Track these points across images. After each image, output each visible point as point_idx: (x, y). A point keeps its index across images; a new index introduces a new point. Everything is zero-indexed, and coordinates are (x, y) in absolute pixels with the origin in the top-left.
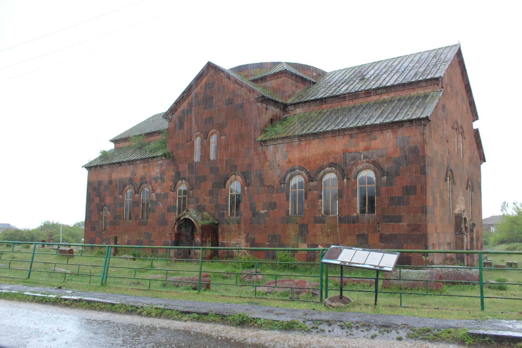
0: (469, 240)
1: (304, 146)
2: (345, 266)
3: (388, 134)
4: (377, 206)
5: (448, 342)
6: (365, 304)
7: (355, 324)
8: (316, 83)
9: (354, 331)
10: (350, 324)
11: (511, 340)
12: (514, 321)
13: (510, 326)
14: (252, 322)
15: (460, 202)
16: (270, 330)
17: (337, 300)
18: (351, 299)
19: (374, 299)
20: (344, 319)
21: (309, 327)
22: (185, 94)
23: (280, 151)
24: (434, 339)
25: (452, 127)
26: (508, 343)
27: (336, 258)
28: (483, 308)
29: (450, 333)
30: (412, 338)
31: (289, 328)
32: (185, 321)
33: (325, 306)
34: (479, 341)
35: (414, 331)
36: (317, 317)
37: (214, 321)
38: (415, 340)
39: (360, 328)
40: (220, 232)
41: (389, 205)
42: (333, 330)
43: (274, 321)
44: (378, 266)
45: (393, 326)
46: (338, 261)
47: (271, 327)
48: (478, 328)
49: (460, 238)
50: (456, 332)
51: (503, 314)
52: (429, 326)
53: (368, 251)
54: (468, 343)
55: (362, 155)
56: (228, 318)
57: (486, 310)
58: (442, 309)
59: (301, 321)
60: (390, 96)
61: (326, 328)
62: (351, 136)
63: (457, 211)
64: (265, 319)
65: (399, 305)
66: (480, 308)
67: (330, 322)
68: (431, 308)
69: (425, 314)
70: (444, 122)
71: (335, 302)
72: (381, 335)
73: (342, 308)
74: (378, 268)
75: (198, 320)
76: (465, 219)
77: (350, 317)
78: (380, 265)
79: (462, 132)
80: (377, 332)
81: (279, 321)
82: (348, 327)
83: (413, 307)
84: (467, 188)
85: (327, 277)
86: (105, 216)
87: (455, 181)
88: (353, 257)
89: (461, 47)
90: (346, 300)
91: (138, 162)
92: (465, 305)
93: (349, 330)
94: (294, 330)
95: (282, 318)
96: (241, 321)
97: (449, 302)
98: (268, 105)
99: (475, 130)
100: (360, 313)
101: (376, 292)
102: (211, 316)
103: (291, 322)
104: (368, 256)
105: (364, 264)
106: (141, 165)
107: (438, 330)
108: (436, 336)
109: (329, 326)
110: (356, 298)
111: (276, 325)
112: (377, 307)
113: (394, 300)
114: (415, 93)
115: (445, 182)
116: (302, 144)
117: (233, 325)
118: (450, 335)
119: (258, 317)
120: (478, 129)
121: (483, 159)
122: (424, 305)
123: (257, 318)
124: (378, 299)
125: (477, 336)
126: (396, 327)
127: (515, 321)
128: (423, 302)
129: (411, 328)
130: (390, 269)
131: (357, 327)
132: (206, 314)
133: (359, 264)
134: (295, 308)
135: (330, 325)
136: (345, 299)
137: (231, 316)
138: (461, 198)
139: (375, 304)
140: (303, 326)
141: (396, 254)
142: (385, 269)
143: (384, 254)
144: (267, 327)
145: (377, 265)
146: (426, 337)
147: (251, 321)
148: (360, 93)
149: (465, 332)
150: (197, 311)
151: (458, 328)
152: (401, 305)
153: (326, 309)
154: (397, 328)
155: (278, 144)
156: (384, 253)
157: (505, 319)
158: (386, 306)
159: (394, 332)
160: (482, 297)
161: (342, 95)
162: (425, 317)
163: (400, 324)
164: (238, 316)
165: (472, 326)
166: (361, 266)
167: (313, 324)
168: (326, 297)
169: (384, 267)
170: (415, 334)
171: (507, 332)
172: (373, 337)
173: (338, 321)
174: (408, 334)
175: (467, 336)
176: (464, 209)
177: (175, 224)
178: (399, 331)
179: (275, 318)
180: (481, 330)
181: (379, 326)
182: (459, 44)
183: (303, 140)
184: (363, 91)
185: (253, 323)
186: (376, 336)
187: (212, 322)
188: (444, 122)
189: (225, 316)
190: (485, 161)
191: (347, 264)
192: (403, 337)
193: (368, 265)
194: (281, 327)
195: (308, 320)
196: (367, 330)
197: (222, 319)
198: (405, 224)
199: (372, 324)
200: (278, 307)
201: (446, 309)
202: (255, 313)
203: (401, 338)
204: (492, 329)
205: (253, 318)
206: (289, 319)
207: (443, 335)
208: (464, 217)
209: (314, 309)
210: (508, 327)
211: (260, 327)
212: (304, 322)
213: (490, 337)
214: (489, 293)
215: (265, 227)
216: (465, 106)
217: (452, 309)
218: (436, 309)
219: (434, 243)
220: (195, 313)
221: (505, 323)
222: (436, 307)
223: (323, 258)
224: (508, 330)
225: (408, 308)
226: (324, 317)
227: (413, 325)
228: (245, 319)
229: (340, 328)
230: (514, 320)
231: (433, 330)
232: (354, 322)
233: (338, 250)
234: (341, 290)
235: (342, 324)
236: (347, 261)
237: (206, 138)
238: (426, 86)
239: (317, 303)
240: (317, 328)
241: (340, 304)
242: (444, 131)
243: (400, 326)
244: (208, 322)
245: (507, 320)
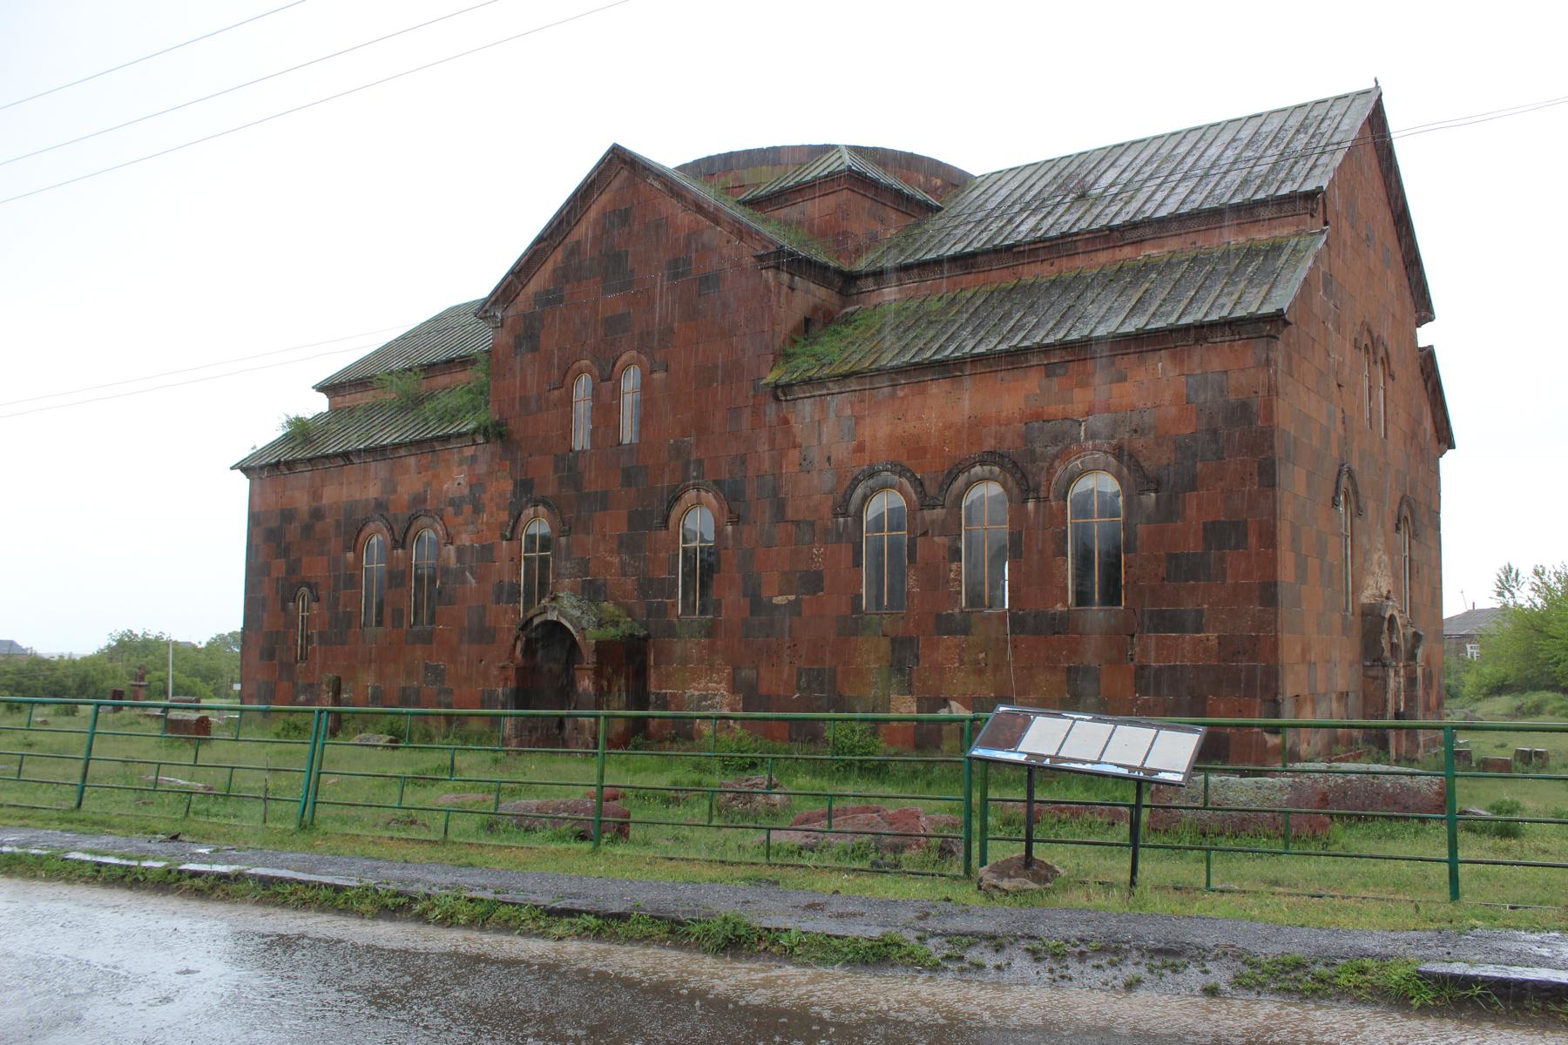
0: (1402, 685)
2: (1040, 767)
3: (1160, 364)
4: (1127, 583)
5: (1357, 1001)
6: (1100, 883)
7: (1075, 946)
8: (941, 209)
9: (1074, 968)
10: (1061, 945)
11: (1548, 994)
12: (1552, 934)
13: (1545, 952)
14: (764, 941)
15: (1377, 570)
16: (819, 964)
17: (1016, 871)
18: (1057, 867)
19: (1128, 866)
20: (1041, 930)
21: (937, 957)
22: (545, 244)
23: (832, 415)
24: (1314, 991)
26: (1539, 1005)
27: (1012, 744)
28: (1455, 894)
29: (1362, 971)
30: (1250, 988)
31: (874, 959)
32: (560, 939)
33: (980, 888)
34: (1450, 998)
35: (1253, 965)
36: (960, 924)
37: (646, 940)
38: (1259, 993)
39: (1092, 957)
40: (652, 663)
41: (1163, 579)
42: (1009, 964)
43: (828, 936)
44: (1141, 769)
45: (1189, 953)
46: (1021, 752)
47: (819, 955)
48: (1447, 958)
49: (1375, 678)
50: (1381, 969)
51: (1517, 912)
52: (1298, 952)
53: (1111, 722)
54: (1418, 1004)
55: (1083, 428)
56: (691, 929)
57: (1466, 898)
58: (1333, 897)
59: (910, 936)
60: (1166, 249)
61: (990, 959)
63: (1366, 597)
64: (804, 933)
65: (1203, 885)
66: (1448, 897)
67: (999, 940)
68: (1298, 895)
69: (1282, 911)
70: (1330, 326)
71: (1010, 877)
72: (1155, 977)
73: (1032, 895)
74: (1142, 774)
75: (598, 935)
76: (1392, 616)
77: (1058, 923)
78: (1148, 765)
79: (1384, 356)
80: (1142, 971)
81: (844, 937)
82: (1055, 955)
83: (1244, 892)
84: (1398, 528)
85: (985, 801)
86: (303, 617)
87: (1361, 504)
88: (1065, 739)
89: (1384, 98)
90: (1043, 872)
91: (403, 452)
92: (1400, 885)
93: (1059, 963)
94: (892, 965)
95: (855, 930)
96: (730, 936)
97: (1352, 875)
98: (797, 278)
99: (1422, 350)
100: (1089, 911)
101: (1135, 843)
102: (639, 923)
103: (883, 940)
104: (1110, 738)
105: (1098, 762)
106: (412, 461)
107: (1326, 965)
108: (1323, 981)
109: (997, 951)
110: (1071, 864)
111: (836, 951)
112: (1137, 891)
113: (1186, 869)
114: (1242, 239)
115: (1333, 510)
116: (900, 394)
117: (705, 951)
118: (1363, 977)
119: (782, 926)
120: (1431, 347)
121: (1445, 439)
122: (1276, 883)
123: (777, 929)
124: (1140, 866)
125: (1445, 983)
126: (1201, 955)
127: (1557, 934)
128: (1271, 875)
129: (1245, 957)
130: (1179, 778)
131: (1082, 953)
132: (622, 917)
133: (1084, 762)
134: (890, 895)
135: (999, 948)
136: (1041, 867)
137: (700, 921)
138: (1380, 557)
139: (1133, 883)
140: (919, 952)
141: (1196, 732)
142: (1162, 776)
143: (1158, 732)
144: (810, 955)
145: (1138, 765)
146: (1291, 985)
147: (760, 939)
148: (1074, 239)
149: (1409, 970)
150: (596, 908)
151: (1387, 957)
152: (1208, 884)
153: (984, 899)
154: (1204, 957)
155: (828, 394)
156: (1160, 727)
157: (1526, 930)
158: (1165, 888)
159: (1193, 970)
160: (1453, 862)
162: (1286, 923)
163: (1211, 945)
164: (719, 922)
165: (1428, 952)
166: (1088, 767)
167: (947, 945)
168: (983, 862)
169: (1161, 771)
170: (1257, 976)
171: (1537, 969)
172: (1130, 986)
173: (1022, 937)
174: (1235, 977)
175: (1415, 984)
176: (1389, 592)
177: (517, 638)
178: (1208, 966)
179: (834, 927)
180: (1460, 964)
181: (1150, 951)
182: (1377, 86)
183: (903, 382)
184: (1083, 234)
185: (767, 944)
186: (1139, 981)
187: (640, 940)
188: (1330, 326)
189: (680, 923)
191: (1047, 761)
192: (1223, 986)
193: (1111, 764)
194: (851, 956)
195: (934, 935)
196: (1113, 964)
197: (672, 932)
198: (1213, 636)
199: (1127, 946)
200: (836, 892)
201: (1343, 898)
202: (772, 913)
203: (1216, 989)
204: (1490, 960)
205: (766, 929)
206: (876, 932)
207: (1342, 980)
208: (1387, 616)
209: (948, 900)
210: (1538, 953)
211: (788, 955)
212: (919, 938)
213: (1485, 985)
214: (1470, 848)
216: (1393, 279)
217: (1363, 898)
218: (1313, 897)
219: (1299, 692)
220: (588, 913)
221: (1528, 941)
222: (1312, 891)
223: (974, 745)
224: (1539, 964)
225: (1229, 896)
226: (979, 925)
227: (1252, 949)
228: (742, 931)
229: (1029, 957)
230: (1553, 931)
231: (1313, 963)
232: (1073, 940)
233: (1020, 721)
234: (1029, 841)
235: (1036, 944)
236: (1046, 753)
237: (609, 379)
238: (1278, 218)
239: (955, 878)
240: (961, 958)
241: (1026, 883)
242: (1329, 355)
243: (1211, 951)
244: (630, 940)
245: (1533, 932)
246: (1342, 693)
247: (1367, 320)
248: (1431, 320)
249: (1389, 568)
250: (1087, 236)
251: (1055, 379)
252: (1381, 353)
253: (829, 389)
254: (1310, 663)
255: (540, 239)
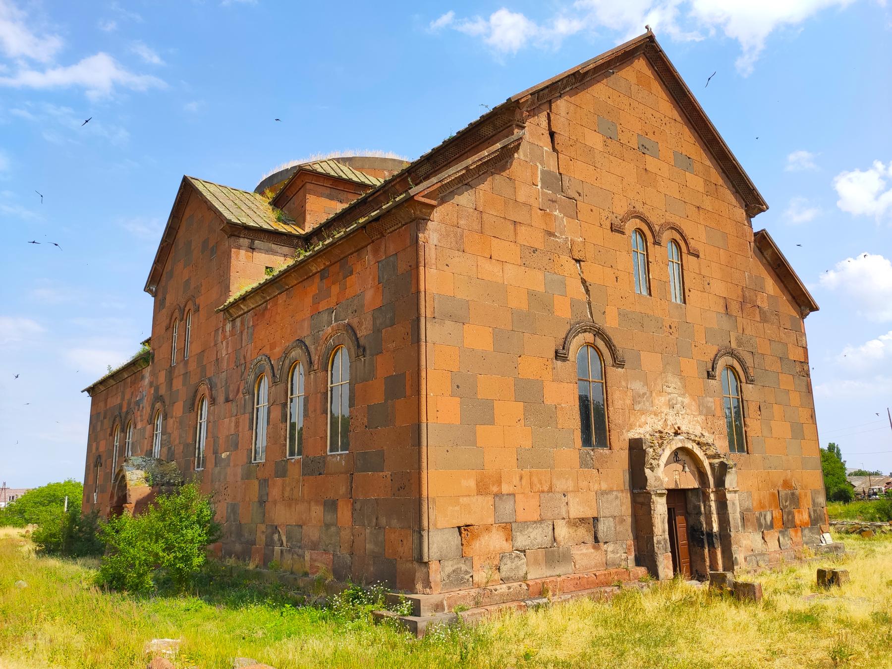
1: (270, 312)
3: (367, 257)
25: (609, 227)
49: (642, 504)
55: (334, 314)
62: (323, 274)
63: (634, 434)
70: (557, 213)
79: (678, 237)
98: (256, 241)
115: (559, 363)
138: (669, 401)
161: (369, 197)
188: (557, 213)
190: (814, 308)
198: (388, 473)
215: (225, 489)
246: (582, 520)
247: (639, 208)
248: (764, 211)
249: (694, 407)
250: (398, 180)
251: (324, 281)
252: (667, 236)
253: (243, 310)
254: (498, 495)
255: (164, 240)
